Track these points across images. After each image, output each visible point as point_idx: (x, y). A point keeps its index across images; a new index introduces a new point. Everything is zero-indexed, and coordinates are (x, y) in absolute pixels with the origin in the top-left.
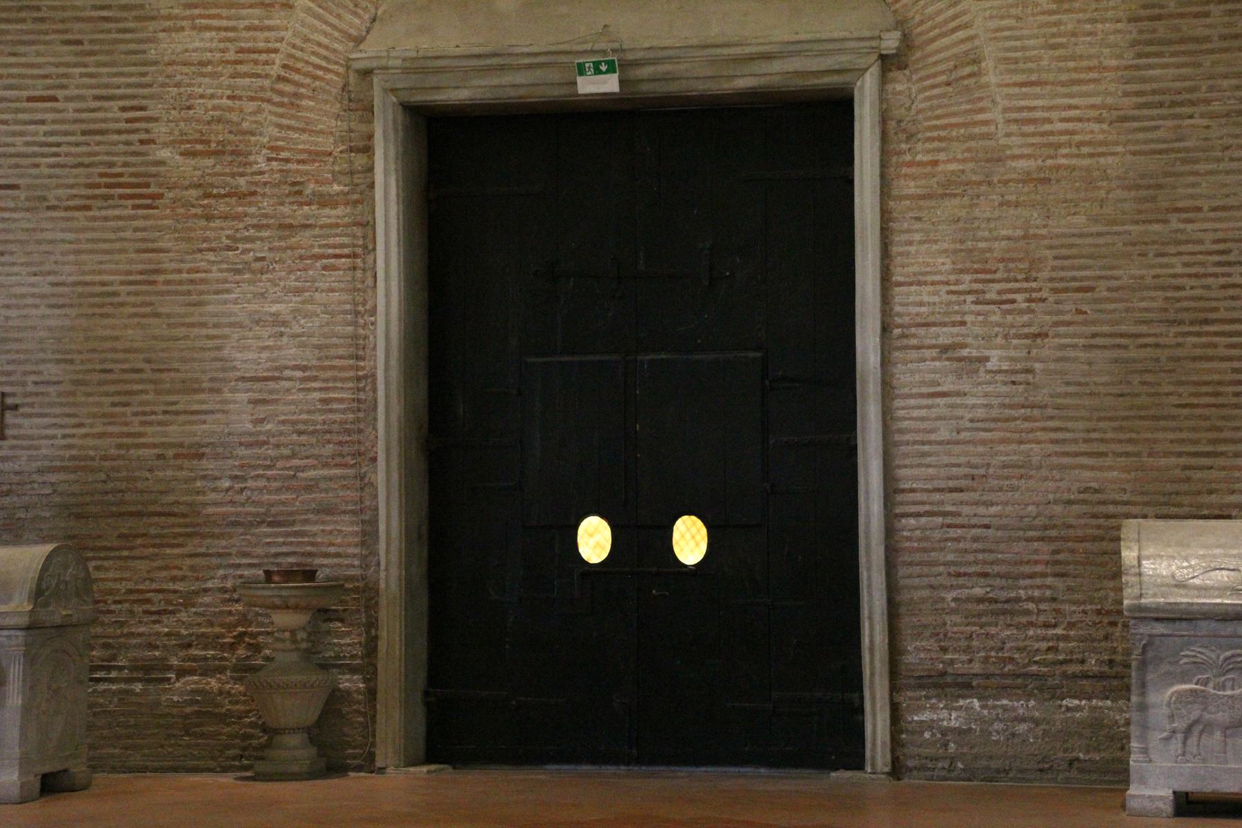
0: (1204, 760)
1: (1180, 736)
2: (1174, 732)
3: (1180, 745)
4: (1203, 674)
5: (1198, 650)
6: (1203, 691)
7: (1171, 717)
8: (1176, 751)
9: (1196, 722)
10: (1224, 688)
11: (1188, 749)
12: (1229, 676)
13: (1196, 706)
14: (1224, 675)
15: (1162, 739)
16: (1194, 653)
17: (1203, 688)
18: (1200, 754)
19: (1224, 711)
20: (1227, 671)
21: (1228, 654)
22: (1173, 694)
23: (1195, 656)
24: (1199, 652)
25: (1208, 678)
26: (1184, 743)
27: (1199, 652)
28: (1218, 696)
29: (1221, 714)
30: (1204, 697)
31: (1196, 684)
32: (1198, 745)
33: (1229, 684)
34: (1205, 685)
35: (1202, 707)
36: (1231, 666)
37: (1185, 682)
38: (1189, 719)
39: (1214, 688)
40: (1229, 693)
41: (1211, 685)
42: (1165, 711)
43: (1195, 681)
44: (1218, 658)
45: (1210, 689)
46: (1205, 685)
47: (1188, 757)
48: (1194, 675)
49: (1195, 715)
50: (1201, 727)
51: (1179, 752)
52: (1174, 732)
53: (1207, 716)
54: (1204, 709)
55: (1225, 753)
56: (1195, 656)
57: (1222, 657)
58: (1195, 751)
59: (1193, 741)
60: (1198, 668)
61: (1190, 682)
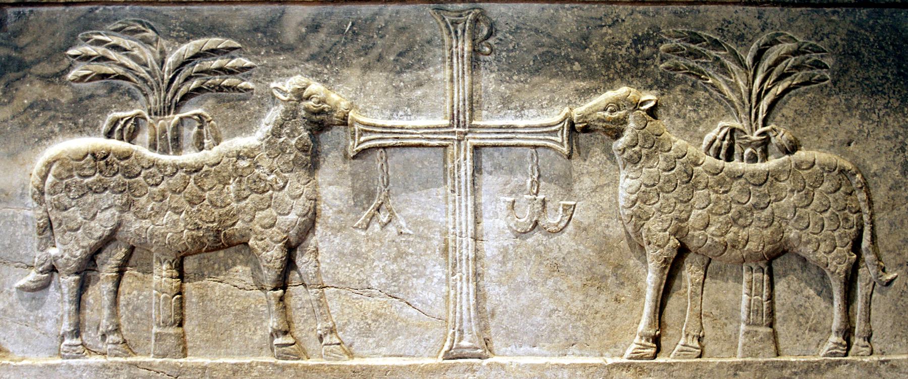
0: (127, 346)
1: (68, 282)
2: (53, 269)
3: (68, 307)
4: (124, 106)
5: (114, 40)
6: (126, 156)
7: (47, 228)
8: (59, 321)
9: (109, 240)
10: (176, 144)
11: (89, 314)
12: (189, 111)
13: (108, 197)
14: (178, 107)
15: (22, 289)
16: (100, 51)
17: (124, 146)
18: (117, 330)
19: (177, 211)
20: (185, 97)
21: (188, 48)
22: (49, 165)
23: (103, 59)
24: (116, 47)
25: (137, 118)
26: (79, 302)
27: (116, 47)
28: (161, 167)
29: (169, 216)
30: (129, 174)
31: (109, 135)
32: (115, 303)
33: (189, 133)
34: (131, 139)
35: (119, 200)
36: (194, 84)
37: (79, 130)
38: (89, 234)
39: (153, 146)
40: (189, 157)
41: (145, 136)
42: (32, 212)
43: (105, 126)
44: (162, 63)
45: (141, 148)
46: (131, 139)
47: (90, 336)
48: (104, 110)
49: (100, 228)
50: (120, 254)
51: (66, 327)
52: (53, 269)
53: (134, 226)
54: (127, 206)
55: (181, 325)
56: (103, 59)
57: (170, 60)
58: (105, 323)
59: (99, 293)
60: (112, 90)
61: (90, 128)
